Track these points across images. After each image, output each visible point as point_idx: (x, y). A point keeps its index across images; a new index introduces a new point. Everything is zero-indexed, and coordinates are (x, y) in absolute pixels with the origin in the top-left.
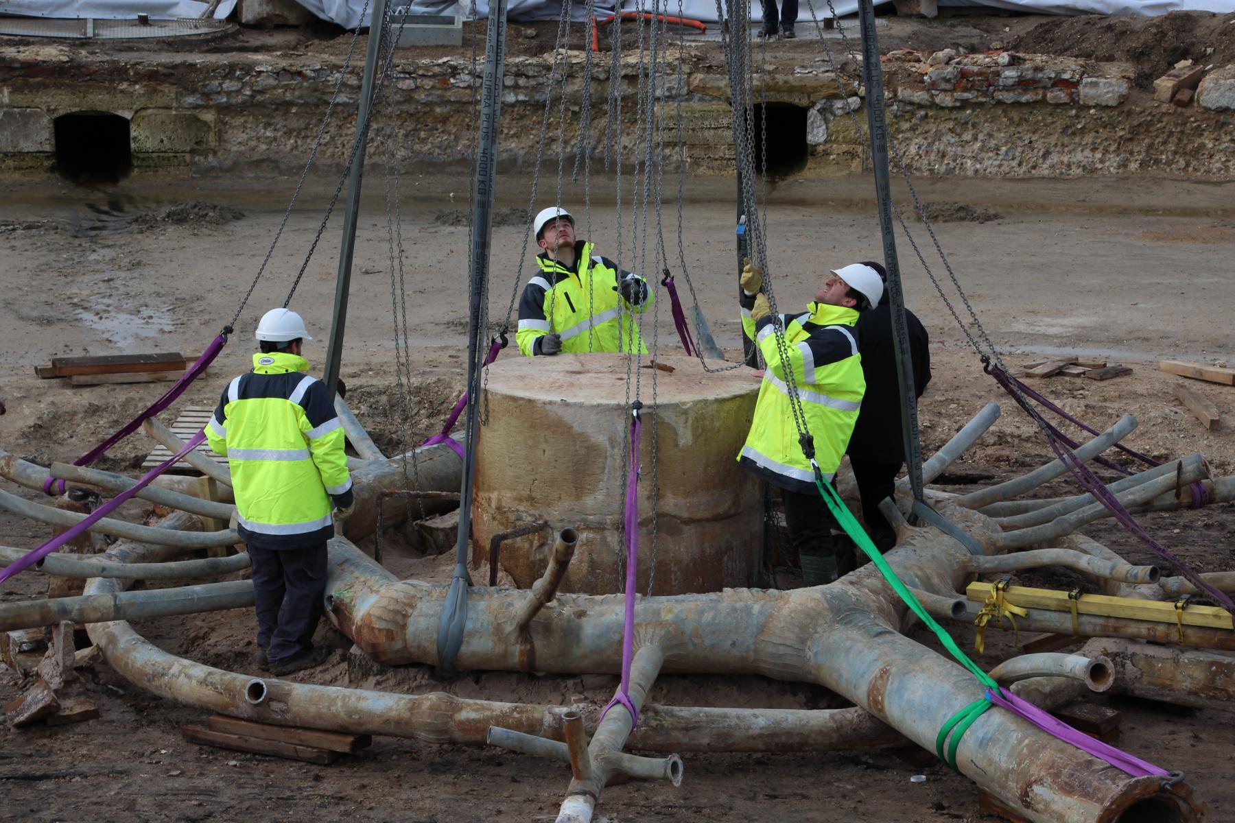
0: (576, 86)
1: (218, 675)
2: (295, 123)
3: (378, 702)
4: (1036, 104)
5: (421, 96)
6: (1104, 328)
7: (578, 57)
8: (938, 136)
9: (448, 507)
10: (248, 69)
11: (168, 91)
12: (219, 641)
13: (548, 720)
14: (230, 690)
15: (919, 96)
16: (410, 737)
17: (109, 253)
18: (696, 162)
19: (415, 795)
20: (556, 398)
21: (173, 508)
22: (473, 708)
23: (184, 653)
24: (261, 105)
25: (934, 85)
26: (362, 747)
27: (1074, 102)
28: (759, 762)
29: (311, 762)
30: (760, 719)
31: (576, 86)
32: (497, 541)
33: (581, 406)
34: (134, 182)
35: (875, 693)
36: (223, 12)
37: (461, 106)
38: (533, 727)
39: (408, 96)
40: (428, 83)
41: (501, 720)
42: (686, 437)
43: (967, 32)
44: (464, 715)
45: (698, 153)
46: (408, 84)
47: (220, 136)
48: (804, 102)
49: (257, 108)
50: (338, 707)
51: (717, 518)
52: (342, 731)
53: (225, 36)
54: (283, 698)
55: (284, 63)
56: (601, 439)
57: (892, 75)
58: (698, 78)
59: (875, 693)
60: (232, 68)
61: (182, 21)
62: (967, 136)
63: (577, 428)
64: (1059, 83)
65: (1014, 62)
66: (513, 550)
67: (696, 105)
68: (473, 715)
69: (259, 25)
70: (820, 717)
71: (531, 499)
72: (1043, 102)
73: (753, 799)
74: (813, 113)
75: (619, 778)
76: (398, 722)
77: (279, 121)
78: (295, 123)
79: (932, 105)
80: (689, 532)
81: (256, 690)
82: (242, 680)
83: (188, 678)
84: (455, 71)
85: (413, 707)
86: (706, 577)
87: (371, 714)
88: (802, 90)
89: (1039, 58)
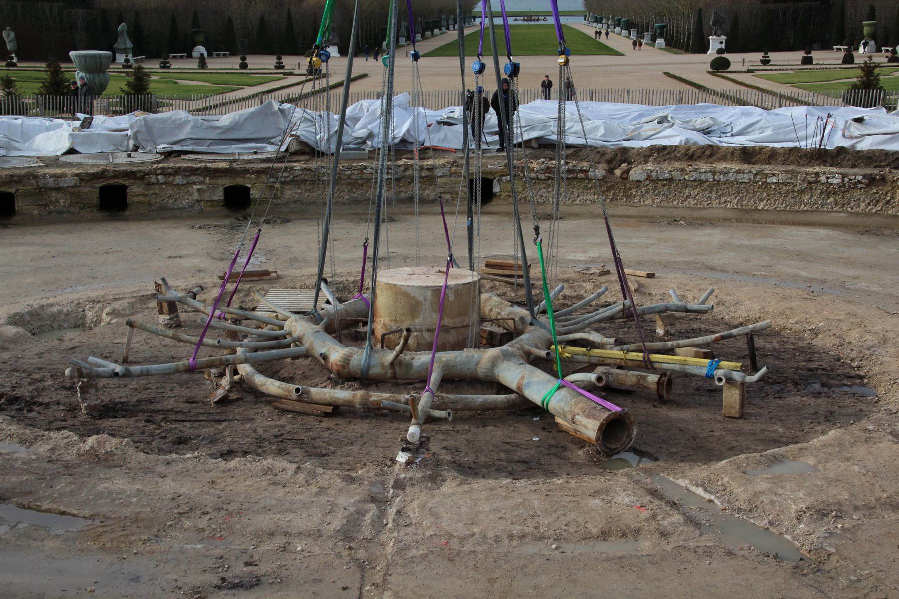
0: (408, 173)
1: (284, 385)
2: (308, 187)
3: (342, 394)
4: (576, 178)
5: (354, 177)
6: (599, 257)
7: (411, 162)
8: (540, 190)
9: (365, 324)
10: (292, 168)
11: (264, 178)
12: (284, 373)
13: (403, 400)
14: (289, 390)
15: (533, 175)
16: (353, 406)
17: (243, 235)
18: (453, 199)
19: (355, 427)
20: (406, 284)
21: (267, 324)
22: (378, 396)
23: (272, 377)
24: (297, 181)
25: (538, 171)
26: (337, 410)
27: (587, 178)
28: (479, 414)
29: (317, 416)
30: (480, 398)
31: (408, 173)
32: (383, 336)
33: (413, 286)
34: (252, 210)
35: (520, 387)
36: (283, 149)
37: (368, 180)
38: (398, 401)
39: (349, 177)
40: (356, 172)
41: (387, 399)
42: (451, 297)
43: (548, 152)
44: (373, 399)
45: (454, 196)
46: (349, 172)
47: (282, 193)
48: (492, 177)
49: (296, 182)
50: (327, 396)
51: (464, 327)
52: (329, 404)
53: (284, 157)
54: (308, 393)
55: (305, 166)
56: (421, 299)
57: (523, 168)
58: (454, 168)
59: (520, 387)
60: (286, 168)
61: (268, 153)
62: (550, 190)
63: (412, 295)
64: (582, 171)
65: (567, 163)
66: (389, 338)
67: (453, 179)
68: (376, 399)
69: (296, 153)
70: (502, 397)
71: (396, 320)
72: (577, 177)
73: (478, 427)
74: (495, 181)
75: (430, 420)
76: (349, 401)
77: (303, 187)
78: (308, 187)
79: (538, 179)
80: (453, 332)
81: (298, 390)
82: (293, 387)
83: (272, 386)
84: (365, 168)
85: (354, 396)
86: (459, 346)
87: (339, 398)
88: (491, 173)
89: (574, 162)
